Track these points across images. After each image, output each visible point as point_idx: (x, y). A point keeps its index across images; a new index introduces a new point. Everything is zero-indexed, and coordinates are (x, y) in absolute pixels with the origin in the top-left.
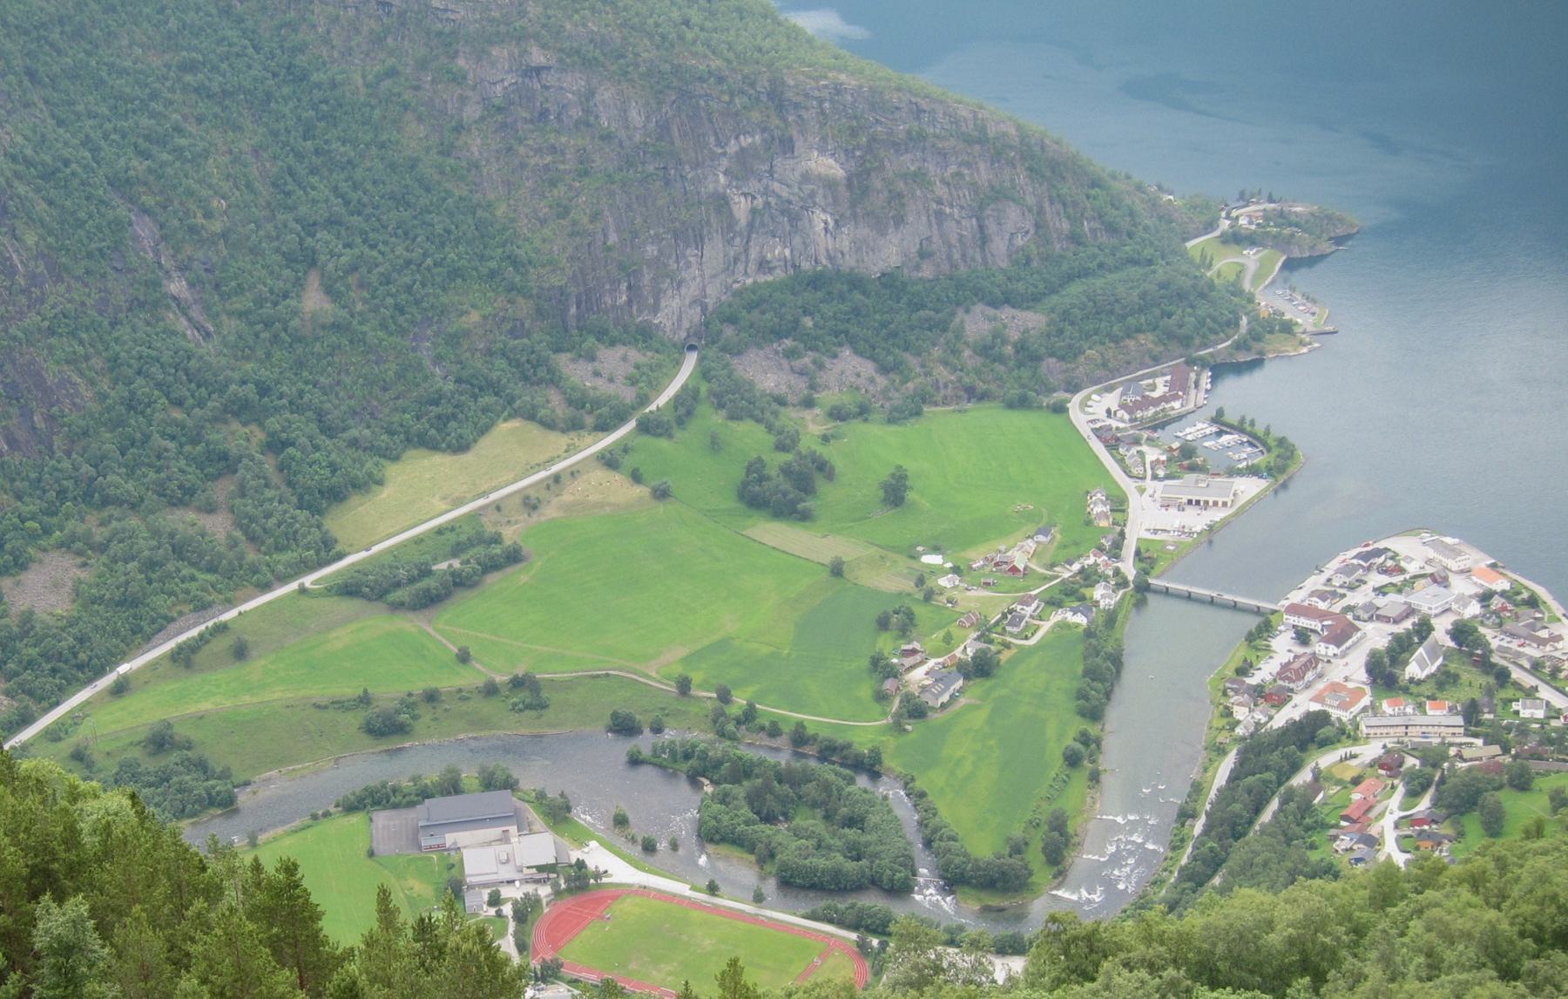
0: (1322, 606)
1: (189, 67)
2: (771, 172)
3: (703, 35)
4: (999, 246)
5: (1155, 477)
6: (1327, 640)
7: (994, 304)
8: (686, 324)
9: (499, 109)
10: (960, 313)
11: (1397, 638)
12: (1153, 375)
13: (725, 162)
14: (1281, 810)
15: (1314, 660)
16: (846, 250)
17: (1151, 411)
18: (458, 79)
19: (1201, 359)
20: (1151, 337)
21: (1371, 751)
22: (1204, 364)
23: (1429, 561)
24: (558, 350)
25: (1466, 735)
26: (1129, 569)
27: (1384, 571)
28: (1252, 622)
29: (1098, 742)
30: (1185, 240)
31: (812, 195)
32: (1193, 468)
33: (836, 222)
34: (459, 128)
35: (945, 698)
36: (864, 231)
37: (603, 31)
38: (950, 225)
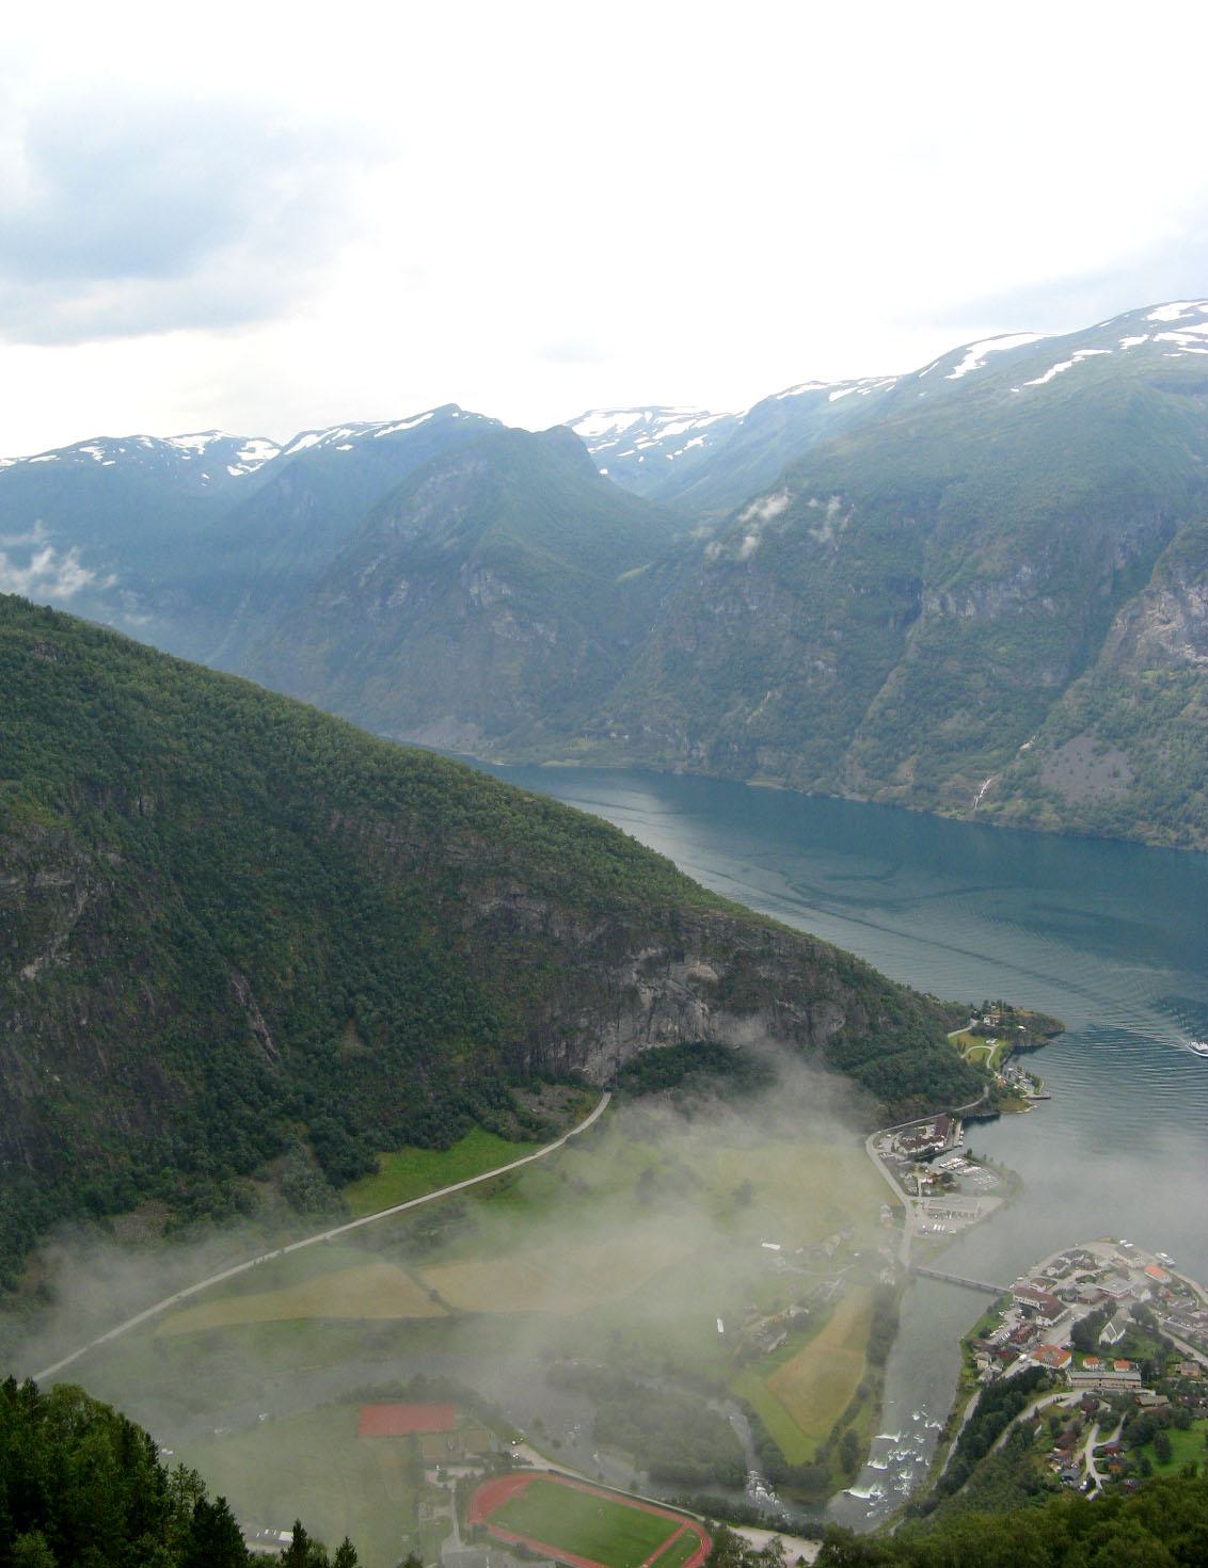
0: (1040, 1290)
1: (281, 878)
2: (668, 974)
3: (626, 880)
5: (925, 1195)
6: (1044, 1315)
9: (486, 920)
11: (1093, 1315)
12: (924, 1124)
15: (1035, 1329)
16: (716, 1029)
17: (923, 1148)
19: (957, 1113)
20: (923, 1096)
21: (1074, 1397)
22: (957, 1117)
23: (1114, 1260)
24: (514, 1085)
25: (1143, 1387)
27: (1084, 1267)
28: (992, 1300)
30: (947, 1032)
32: (949, 1189)
33: (710, 1009)
34: (459, 932)
35: (773, 1346)
37: (560, 874)
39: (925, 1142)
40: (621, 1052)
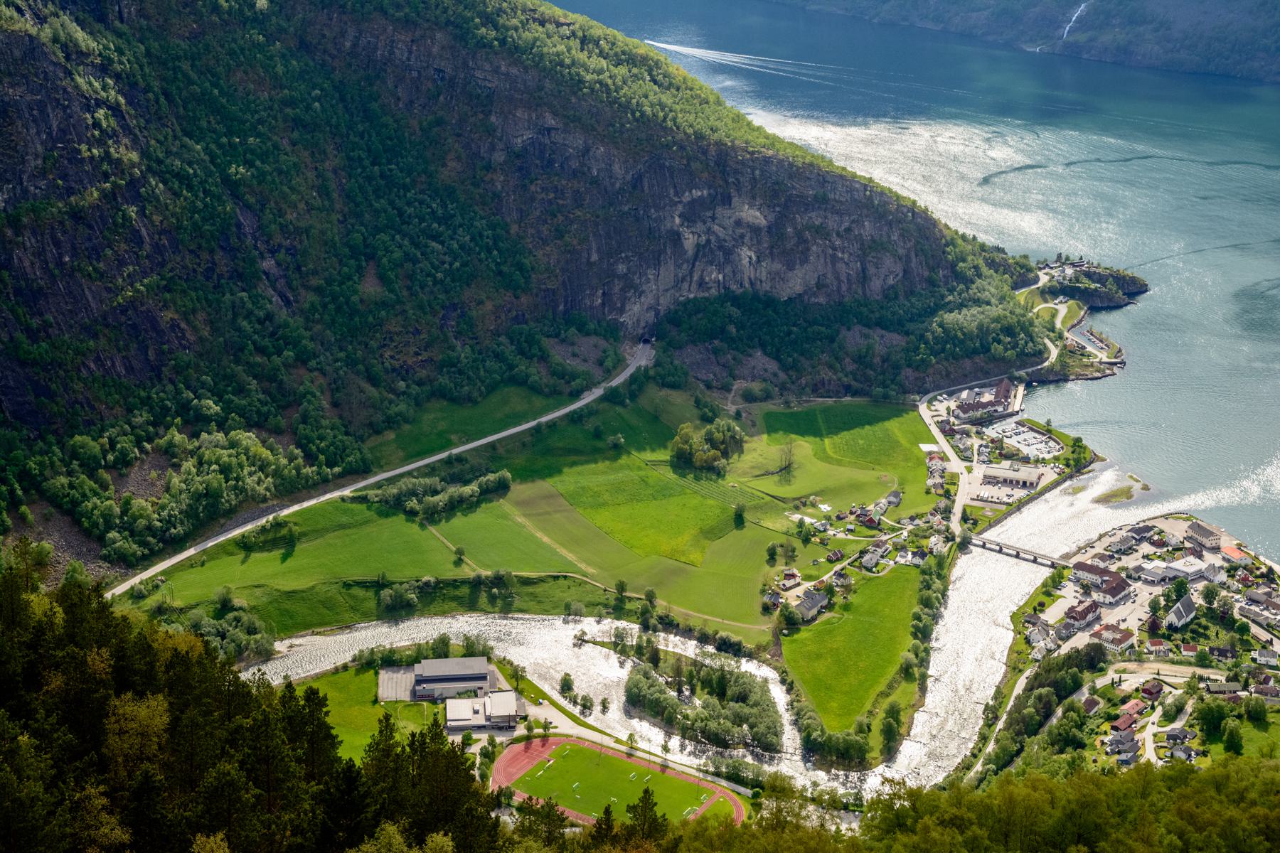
0: (1102, 565)
1: (291, 103)
2: (713, 218)
4: (876, 285)
7: (868, 326)
8: (643, 324)
9: (518, 156)
10: (844, 332)
13: (680, 208)
14: (1064, 716)
18: (490, 131)
26: (956, 527)
27: (1153, 543)
28: (1046, 572)
29: (927, 651)
31: (742, 236)
36: (777, 266)
38: (841, 266)
39: (985, 405)
40: (661, 301)
